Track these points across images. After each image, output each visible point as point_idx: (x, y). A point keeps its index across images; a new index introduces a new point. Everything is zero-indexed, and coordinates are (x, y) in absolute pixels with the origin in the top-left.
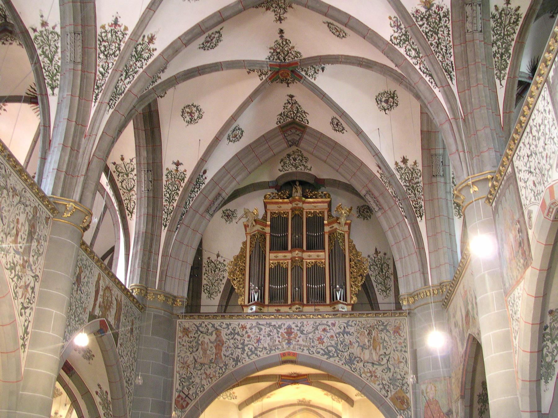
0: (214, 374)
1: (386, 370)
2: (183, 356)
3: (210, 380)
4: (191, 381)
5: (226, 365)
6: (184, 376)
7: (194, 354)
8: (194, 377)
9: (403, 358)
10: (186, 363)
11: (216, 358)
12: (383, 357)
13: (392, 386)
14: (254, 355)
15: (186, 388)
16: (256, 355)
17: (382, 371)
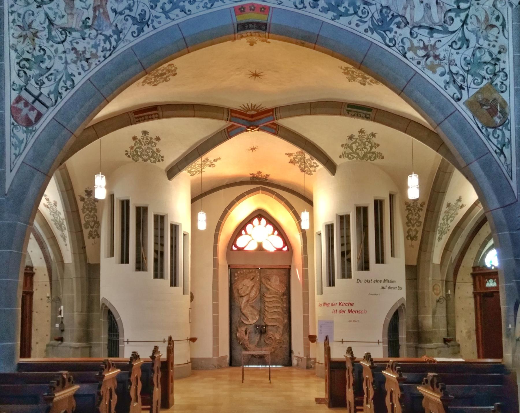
0: (94, 51)
1: (459, 44)
2: (21, 11)
3: (84, 63)
4: (43, 66)
5: (118, 32)
6: (27, 56)
7: (45, 7)
8: (50, 58)
9: (498, 18)
10: (30, 26)
11: (95, 17)
12: (452, 14)
13: (470, 78)
14: (177, 11)
15: (32, 82)
16: (183, 10)
17: (451, 46)
